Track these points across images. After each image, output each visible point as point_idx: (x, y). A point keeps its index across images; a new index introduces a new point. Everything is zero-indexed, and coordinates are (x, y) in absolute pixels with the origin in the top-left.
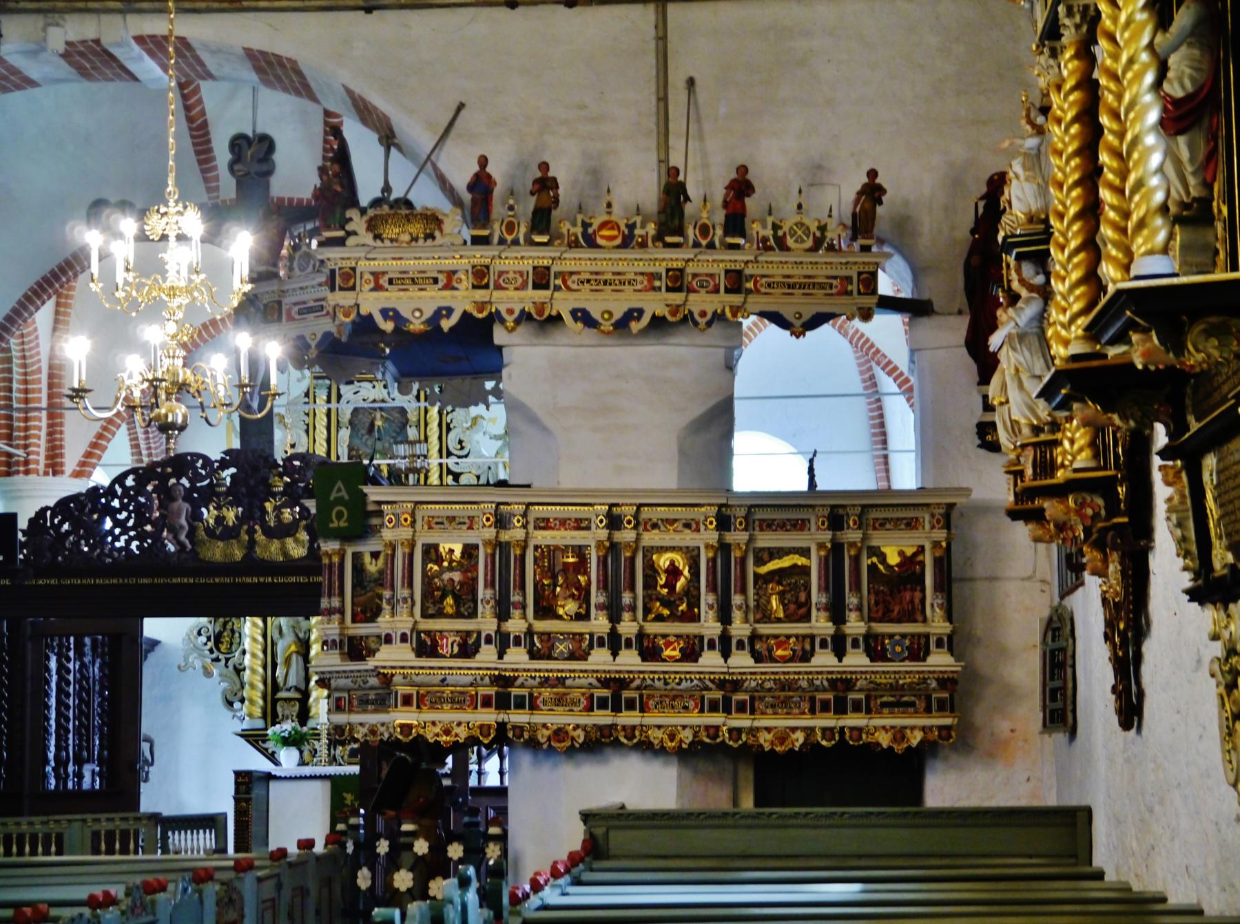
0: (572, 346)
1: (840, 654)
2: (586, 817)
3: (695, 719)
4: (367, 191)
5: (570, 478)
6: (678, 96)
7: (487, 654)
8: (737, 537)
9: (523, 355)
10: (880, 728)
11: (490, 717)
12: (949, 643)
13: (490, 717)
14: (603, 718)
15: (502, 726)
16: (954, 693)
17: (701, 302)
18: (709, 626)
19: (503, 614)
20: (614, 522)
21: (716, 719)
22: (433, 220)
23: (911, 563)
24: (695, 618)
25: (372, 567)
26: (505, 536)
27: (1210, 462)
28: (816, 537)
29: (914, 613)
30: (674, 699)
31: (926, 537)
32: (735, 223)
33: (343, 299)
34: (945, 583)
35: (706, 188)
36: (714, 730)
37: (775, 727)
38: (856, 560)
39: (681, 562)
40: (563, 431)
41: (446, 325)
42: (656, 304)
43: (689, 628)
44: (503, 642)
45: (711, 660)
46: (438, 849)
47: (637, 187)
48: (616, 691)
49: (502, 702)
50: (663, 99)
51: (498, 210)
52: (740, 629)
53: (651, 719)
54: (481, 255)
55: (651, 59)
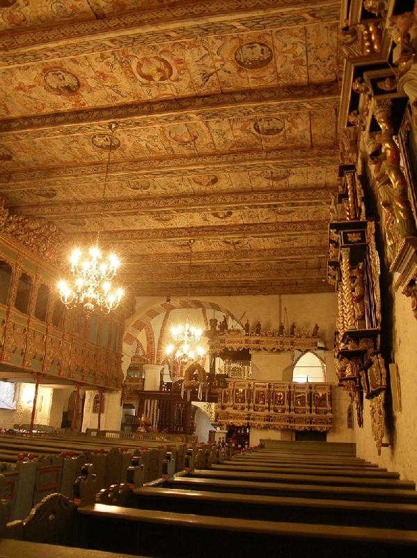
0: (263, 354)
1: (311, 412)
2: (261, 440)
3: (284, 423)
4: (230, 327)
5: (263, 378)
6: (283, 310)
7: (246, 410)
8: (292, 390)
9: (256, 358)
10: (318, 427)
11: (246, 421)
12: (331, 411)
13: (246, 421)
14: (267, 423)
15: (248, 423)
16: (333, 421)
17: (286, 347)
18: (287, 406)
19: (249, 403)
20: (270, 386)
21: (288, 424)
22: (238, 331)
23: (324, 396)
24: (283, 404)
25: (227, 393)
26: (250, 388)
27: (369, 371)
28: (307, 391)
29: (325, 405)
30: (279, 420)
31: (327, 391)
32: (292, 333)
33: (223, 345)
34: (331, 400)
35: (287, 328)
36: (287, 426)
37: (297, 426)
38: (314, 395)
39: (282, 394)
40: (262, 370)
41: (240, 350)
42: (278, 347)
43: (283, 406)
44: (249, 408)
45: (287, 413)
46: (236, 446)
47: (275, 326)
48: (269, 418)
49: (248, 419)
50: (280, 312)
51: (250, 330)
52: (292, 407)
53: (275, 423)
54: (247, 338)
55: (278, 305)
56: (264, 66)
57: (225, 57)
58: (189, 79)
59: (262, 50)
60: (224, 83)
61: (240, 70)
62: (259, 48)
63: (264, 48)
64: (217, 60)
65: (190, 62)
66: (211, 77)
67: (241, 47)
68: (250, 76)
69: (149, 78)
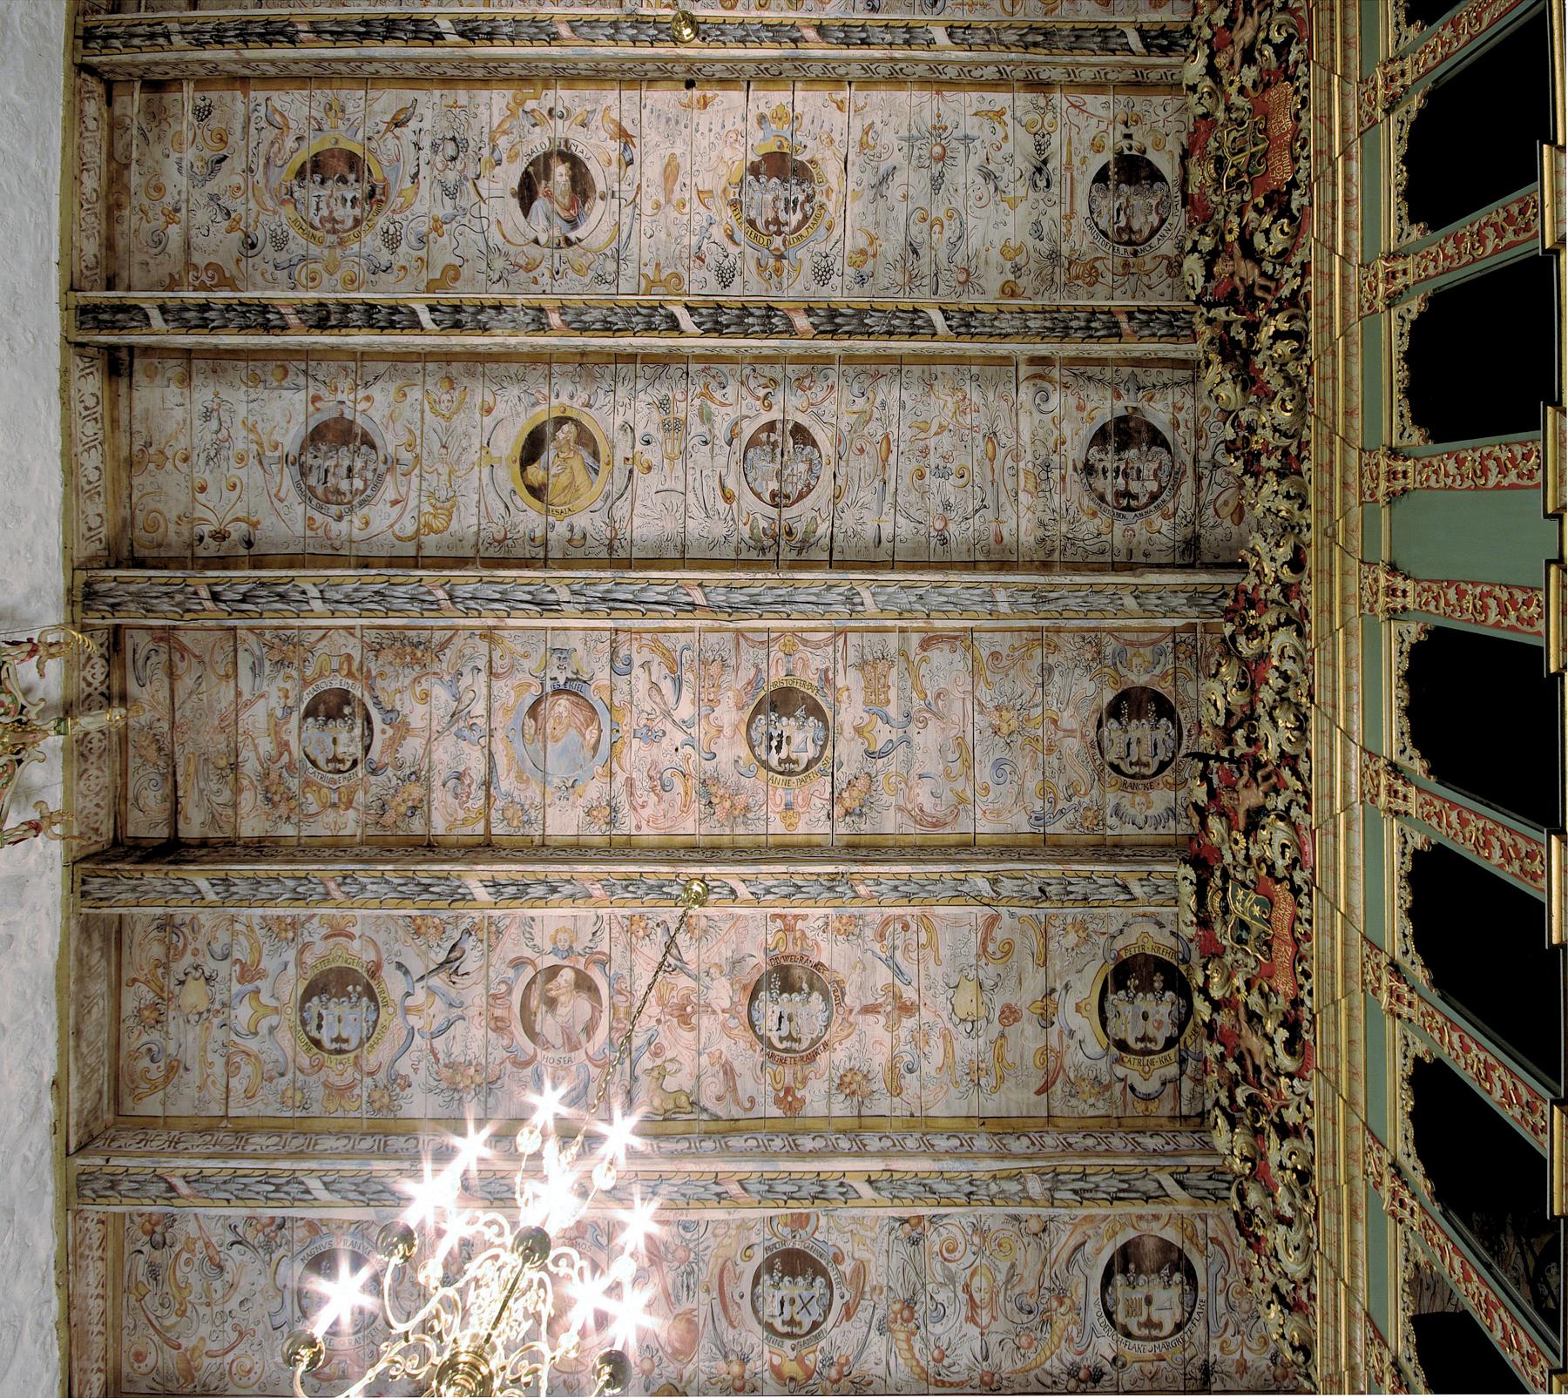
56: (322, 973)
57: (398, 1021)
58: (494, 960)
59: (319, 1027)
60: (417, 932)
61: (375, 971)
62: (325, 1037)
63: (314, 1034)
64: (418, 1010)
65: (477, 1020)
66: (442, 957)
67: (361, 1044)
68: (356, 945)
69: (584, 984)
